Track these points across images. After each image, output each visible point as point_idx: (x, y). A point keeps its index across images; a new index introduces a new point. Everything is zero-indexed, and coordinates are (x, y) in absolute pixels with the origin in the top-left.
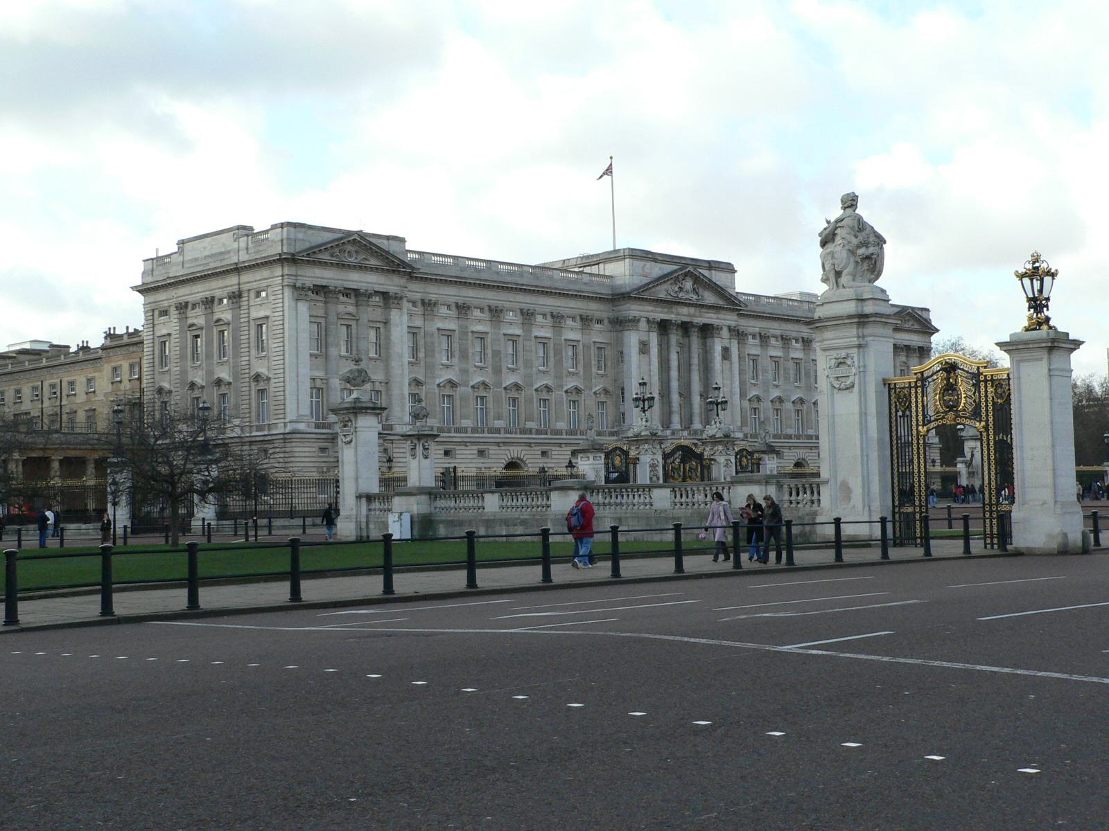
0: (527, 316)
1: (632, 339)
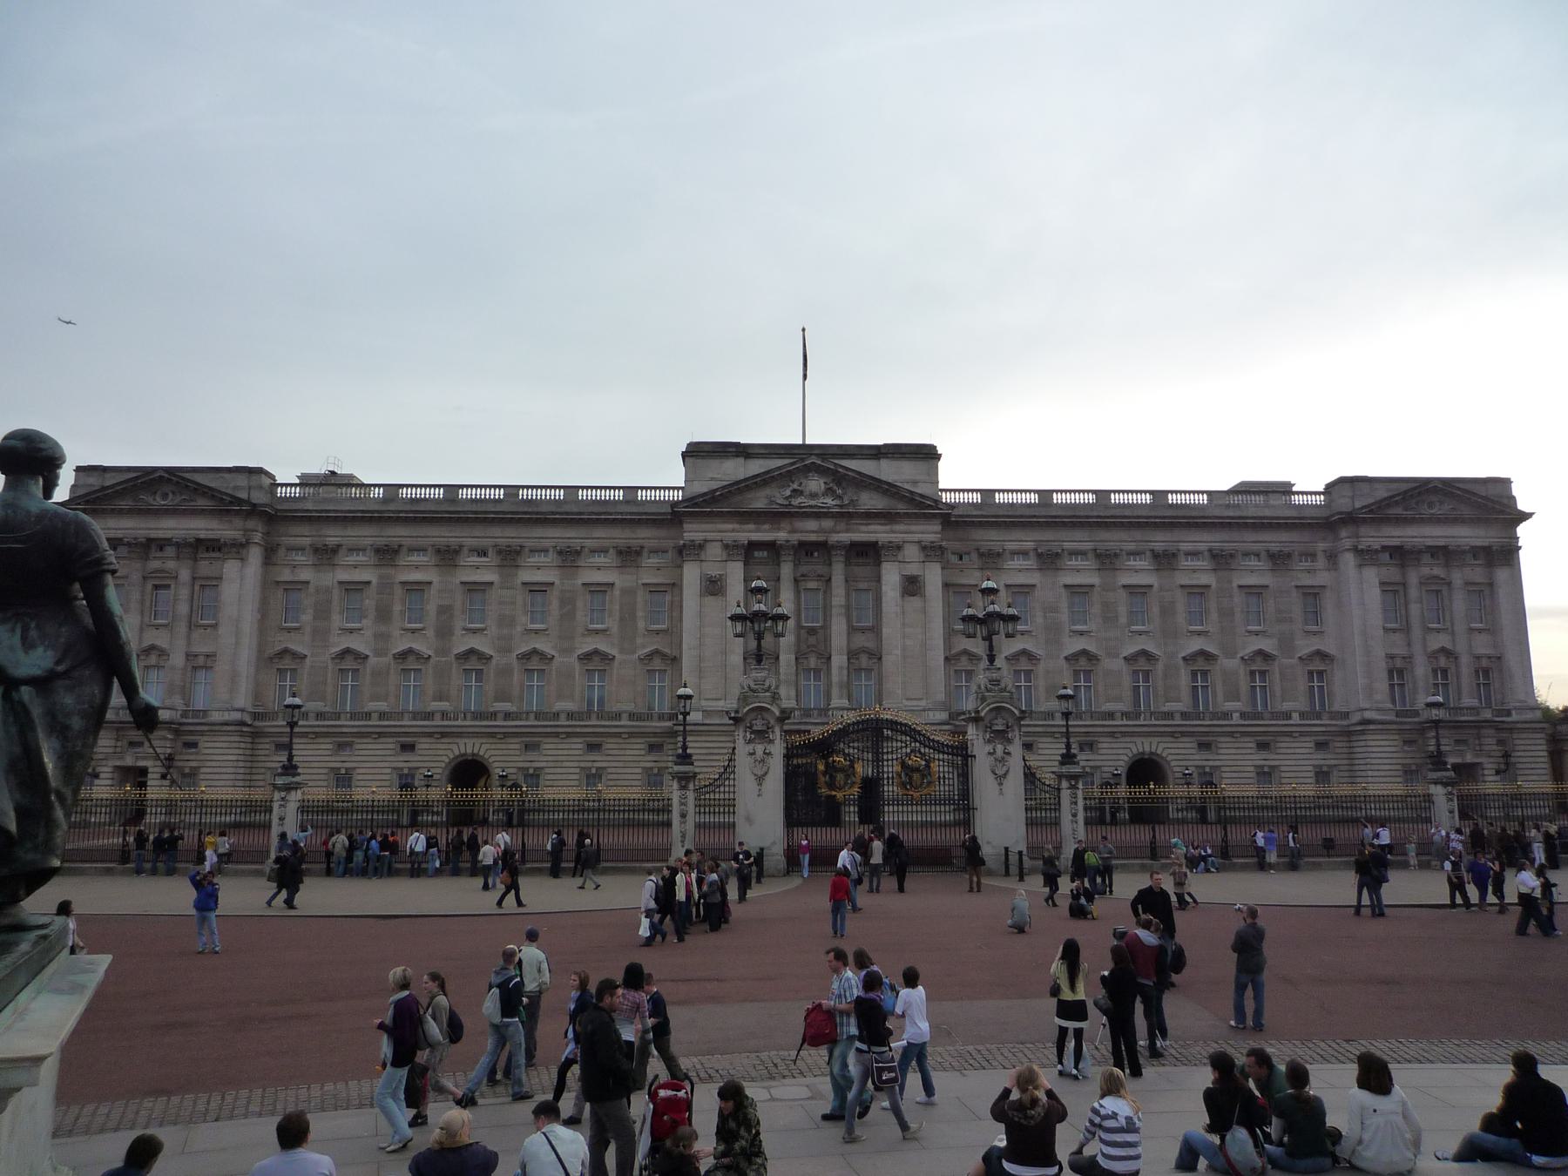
1: (691, 574)
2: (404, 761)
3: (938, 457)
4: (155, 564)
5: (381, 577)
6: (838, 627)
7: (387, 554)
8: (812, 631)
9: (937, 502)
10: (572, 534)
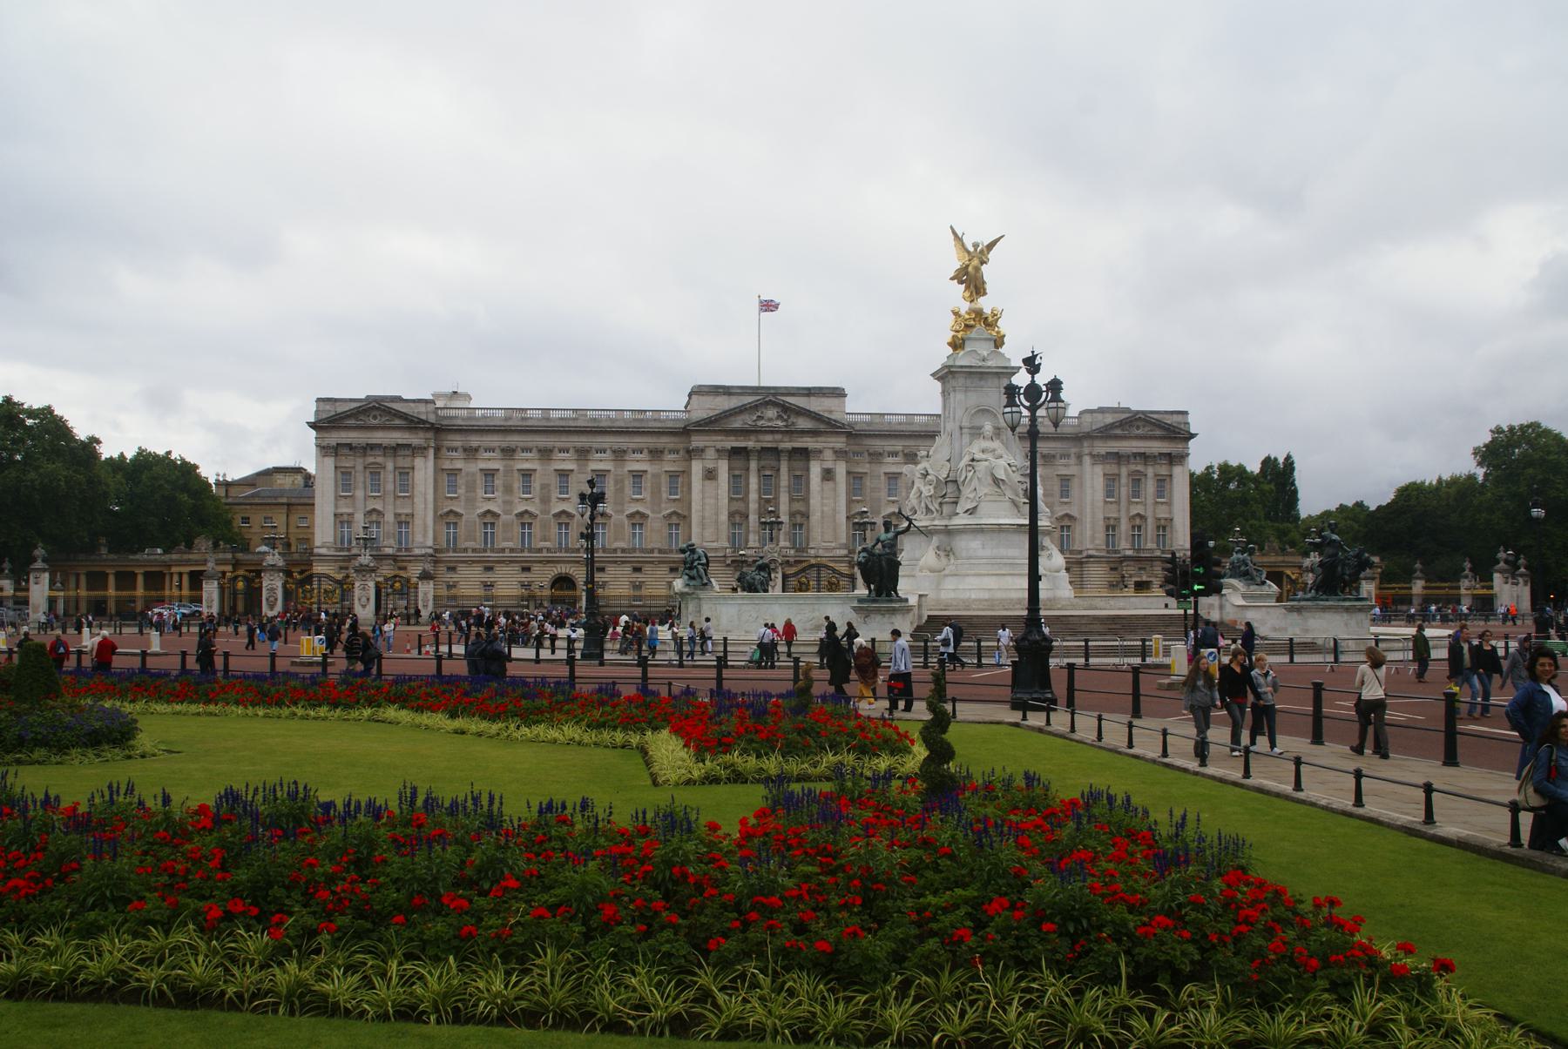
1: (697, 467)
2: (525, 577)
4: (371, 460)
6: (784, 498)
7: (508, 452)
8: (768, 501)
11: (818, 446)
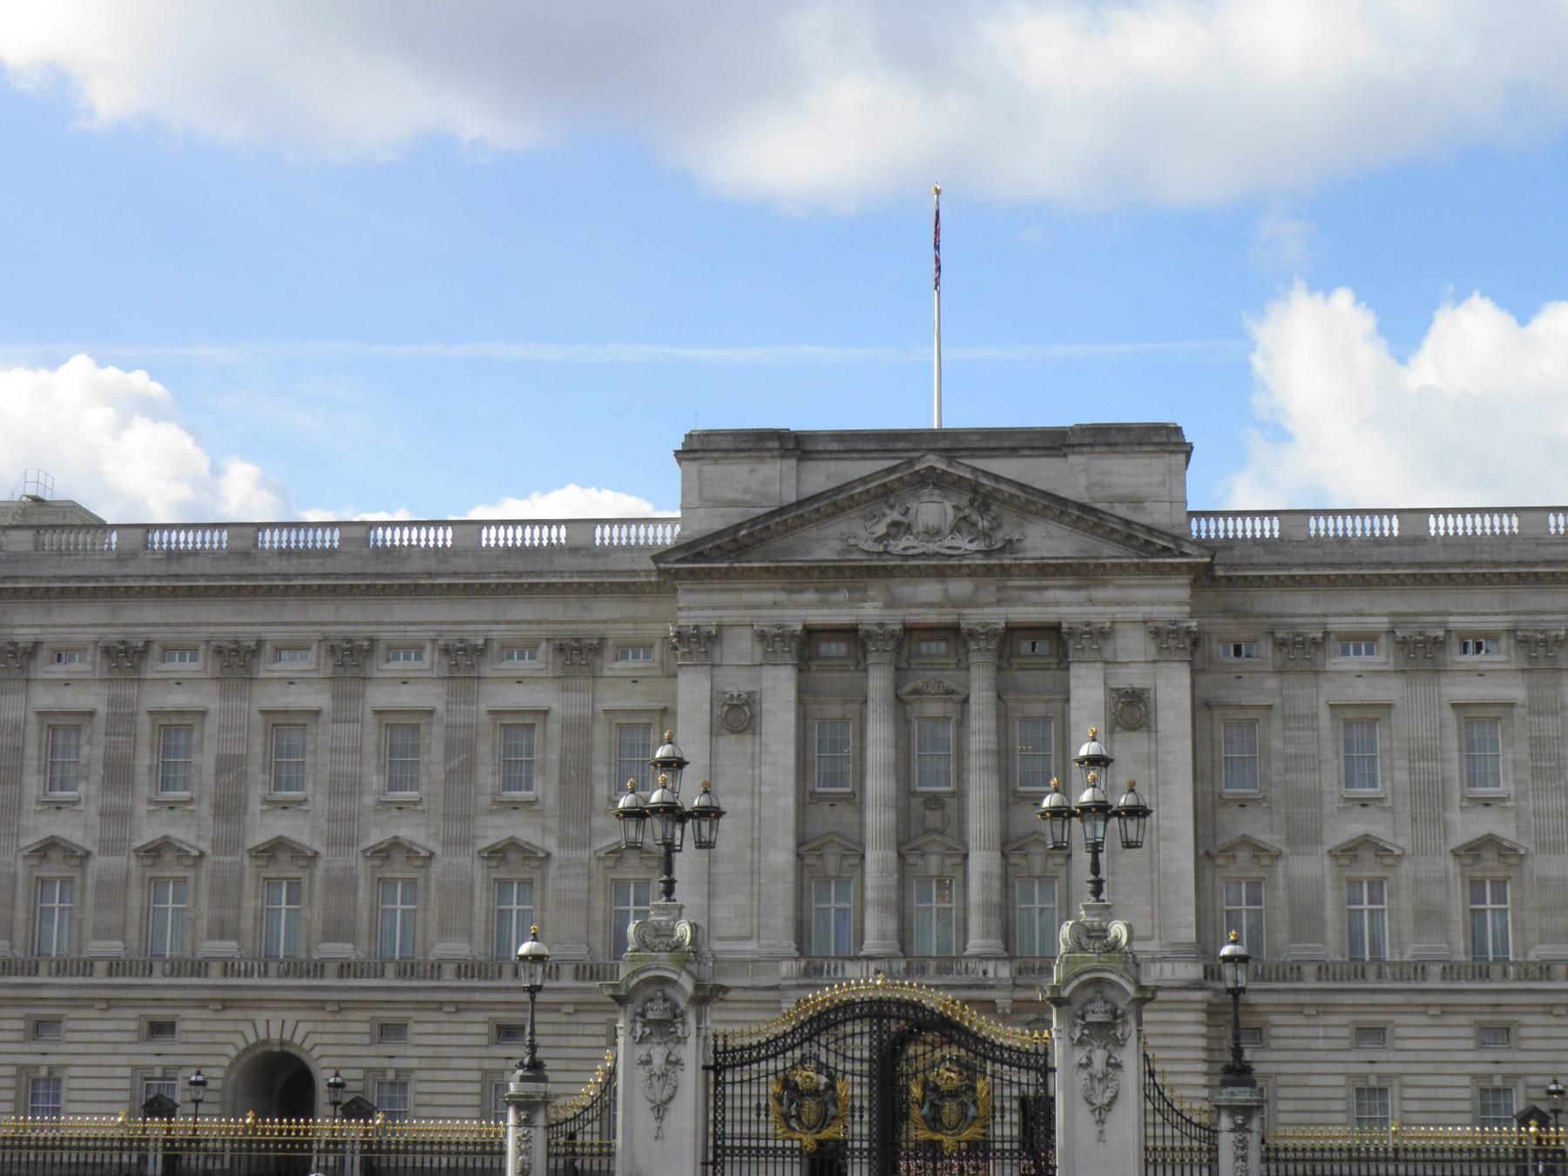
0: (352, 658)
1: (693, 693)
2: (152, 1055)
3: (1187, 451)
5: (111, 703)
6: (981, 793)
7: (126, 658)
8: (935, 801)
9: (1178, 540)
10: (474, 618)
11: (1097, 614)
